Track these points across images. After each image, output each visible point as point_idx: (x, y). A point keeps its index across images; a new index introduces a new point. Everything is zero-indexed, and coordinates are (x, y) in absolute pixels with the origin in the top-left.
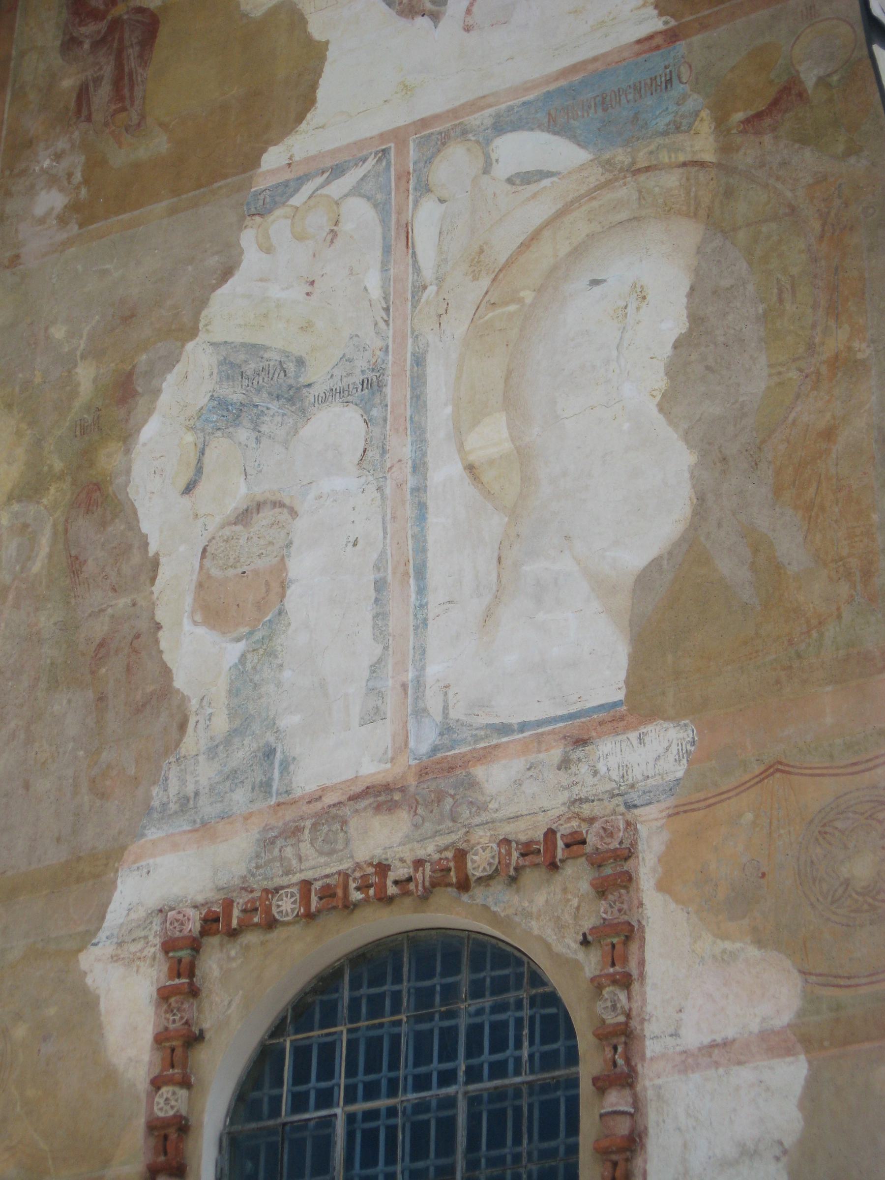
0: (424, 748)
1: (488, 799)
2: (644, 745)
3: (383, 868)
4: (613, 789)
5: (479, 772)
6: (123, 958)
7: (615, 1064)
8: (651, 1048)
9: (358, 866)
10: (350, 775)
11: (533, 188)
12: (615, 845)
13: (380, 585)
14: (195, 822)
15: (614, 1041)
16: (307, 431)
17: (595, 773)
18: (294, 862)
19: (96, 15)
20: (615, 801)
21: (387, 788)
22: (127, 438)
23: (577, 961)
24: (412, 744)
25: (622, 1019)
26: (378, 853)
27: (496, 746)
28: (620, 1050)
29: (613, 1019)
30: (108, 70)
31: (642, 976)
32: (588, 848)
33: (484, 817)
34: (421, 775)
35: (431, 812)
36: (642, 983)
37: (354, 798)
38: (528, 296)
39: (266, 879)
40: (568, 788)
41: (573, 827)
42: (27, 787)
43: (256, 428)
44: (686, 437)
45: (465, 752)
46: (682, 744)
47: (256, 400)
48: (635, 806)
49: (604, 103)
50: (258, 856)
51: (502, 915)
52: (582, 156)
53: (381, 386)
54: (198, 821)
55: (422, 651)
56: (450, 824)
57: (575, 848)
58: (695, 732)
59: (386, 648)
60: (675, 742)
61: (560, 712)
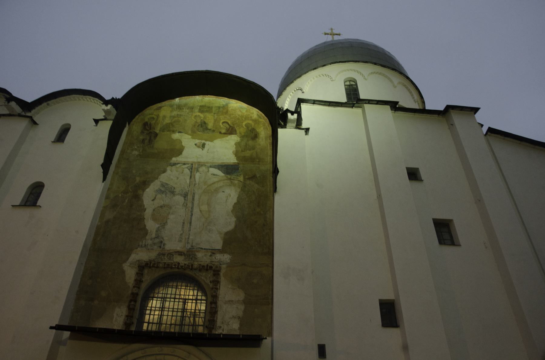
0: (188, 248)
3: (179, 263)
5: (197, 254)
7: (214, 300)
8: (220, 299)
11: (215, 176)
12: (217, 269)
13: (184, 223)
17: (215, 258)
21: (181, 252)
22: (144, 190)
24: (186, 247)
28: (215, 298)
30: (148, 138)
31: (219, 289)
33: (197, 260)
37: (176, 252)
43: (166, 195)
47: (166, 191)
50: (157, 256)
52: (223, 175)
53: (187, 195)
59: (183, 232)
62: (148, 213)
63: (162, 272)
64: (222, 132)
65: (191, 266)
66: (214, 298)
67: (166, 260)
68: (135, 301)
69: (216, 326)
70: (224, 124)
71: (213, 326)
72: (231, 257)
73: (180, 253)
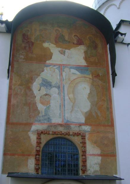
0: (65, 122)
3: (61, 132)
8: (87, 153)
10: (57, 122)
13: (60, 106)
16: (52, 89)
18: (51, 129)
19: (26, 40)
21: (61, 125)
22: (32, 83)
29: (84, 150)
37: (58, 125)
38: (75, 84)
42: (21, 114)
43: (47, 87)
44: (90, 102)
49: (81, 70)
53: (60, 88)
55: (65, 113)
61: (79, 122)
62: (38, 99)
63: (52, 137)
64: (75, 43)
67: (54, 129)
68: (39, 155)
69: (87, 169)
70: (75, 37)
71: (85, 169)
72: (91, 127)
73: (61, 125)
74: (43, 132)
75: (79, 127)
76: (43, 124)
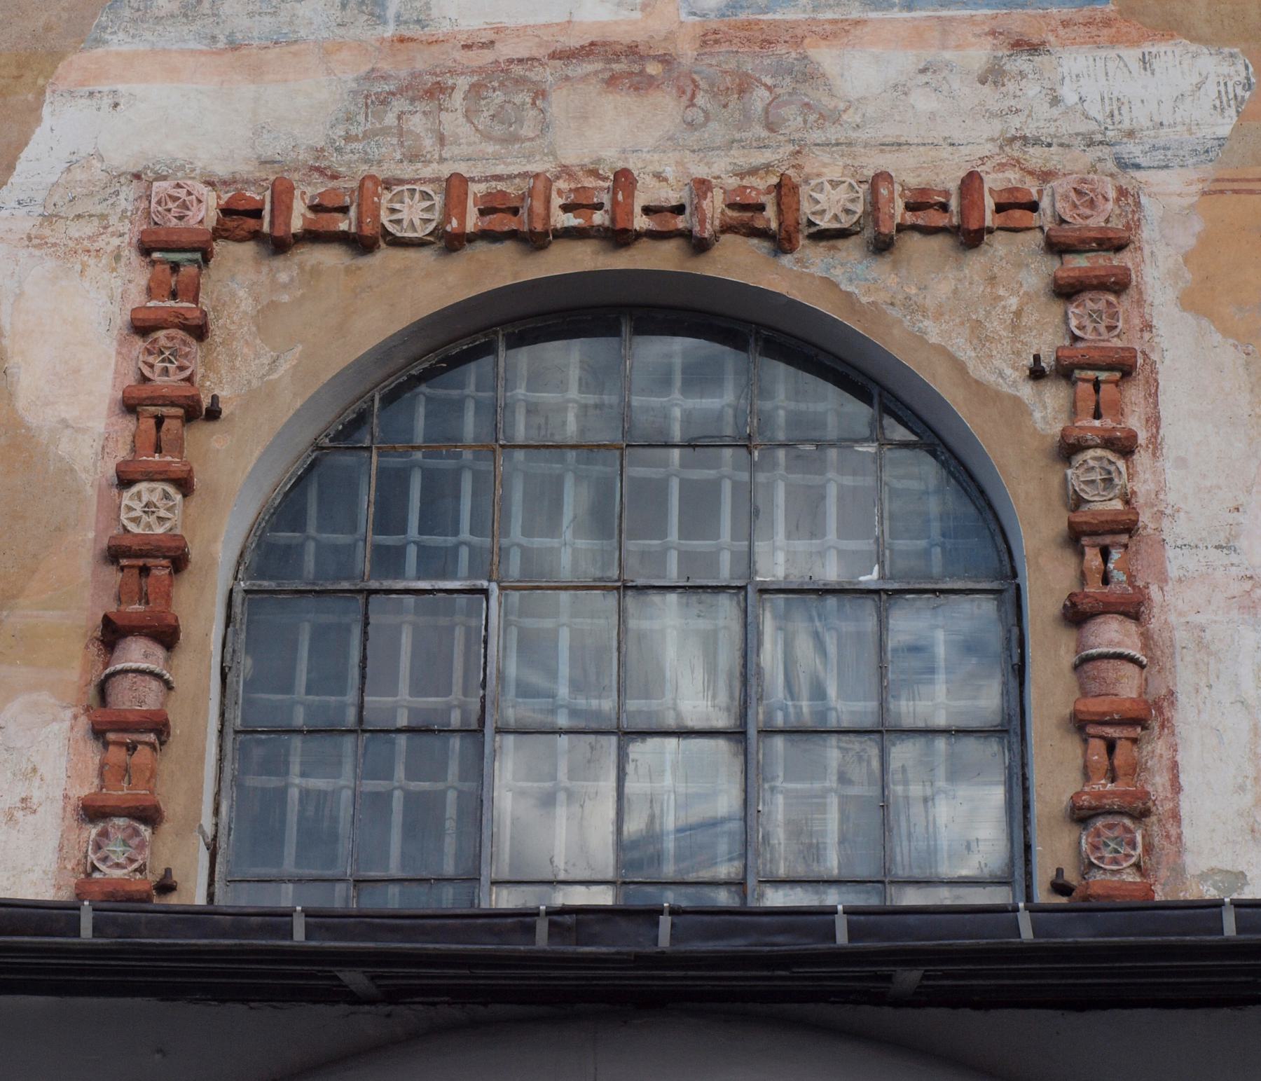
1: (842, 106)
2: (1153, 74)
3: (624, 179)
4: (1093, 133)
5: (825, 57)
6: (54, 245)
7: (1106, 580)
8: (1176, 562)
9: (566, 171)
10: (558, 17)
12: (1097, 221)
14: (214, 38)
15: (1107, 540)
17: (1055, 101)
18: (428, 143)
20: (1094, 153)
21: (633, 51)
23: (1017, 401)
25: (1118, 505)
26: (612, 159)
27: (857, 23)
28: (1116, 555)
31: (1155, 444)
32: (1044, 217)
33: (833, 133)
34: (705, 43)
35: (725, 106)
36: (1155, 448)
39: (366, 161)
40: (1000, 115)
41: (1010, 180)
45: (796, 21)
46: (1225, 84)
48: (1138, 167)
51: (864, 300)
54: (222, 38)
56: (764, 133)
57: (1017, 213)
58: (1251, 69)
60: (1212, 79)
65: (769, 201)
66: (1105, 554)
68: (167, 637)
74: (257, 214)
75: (993, 75)
76: (256, 72)
